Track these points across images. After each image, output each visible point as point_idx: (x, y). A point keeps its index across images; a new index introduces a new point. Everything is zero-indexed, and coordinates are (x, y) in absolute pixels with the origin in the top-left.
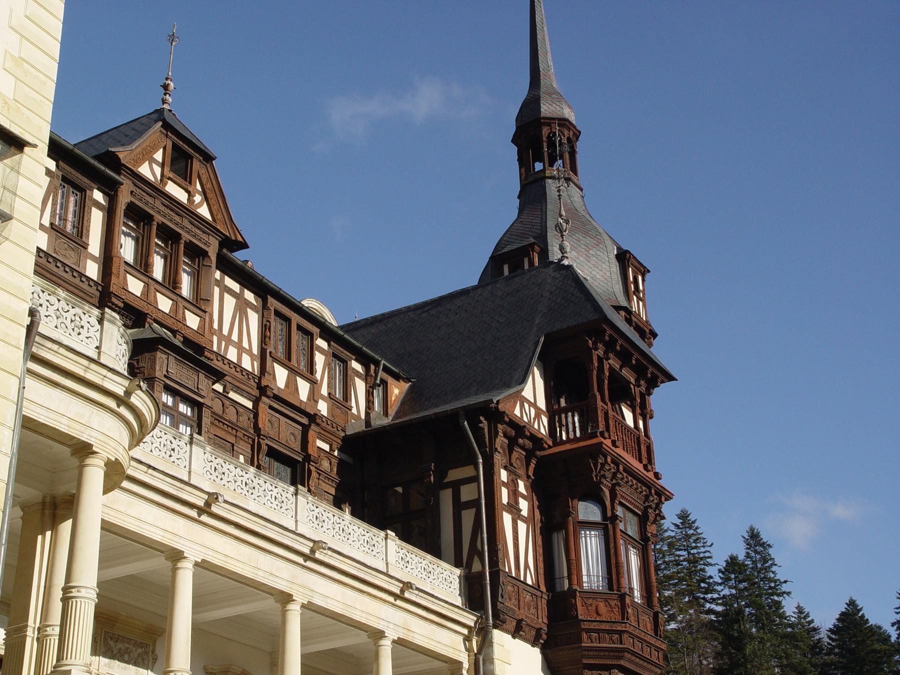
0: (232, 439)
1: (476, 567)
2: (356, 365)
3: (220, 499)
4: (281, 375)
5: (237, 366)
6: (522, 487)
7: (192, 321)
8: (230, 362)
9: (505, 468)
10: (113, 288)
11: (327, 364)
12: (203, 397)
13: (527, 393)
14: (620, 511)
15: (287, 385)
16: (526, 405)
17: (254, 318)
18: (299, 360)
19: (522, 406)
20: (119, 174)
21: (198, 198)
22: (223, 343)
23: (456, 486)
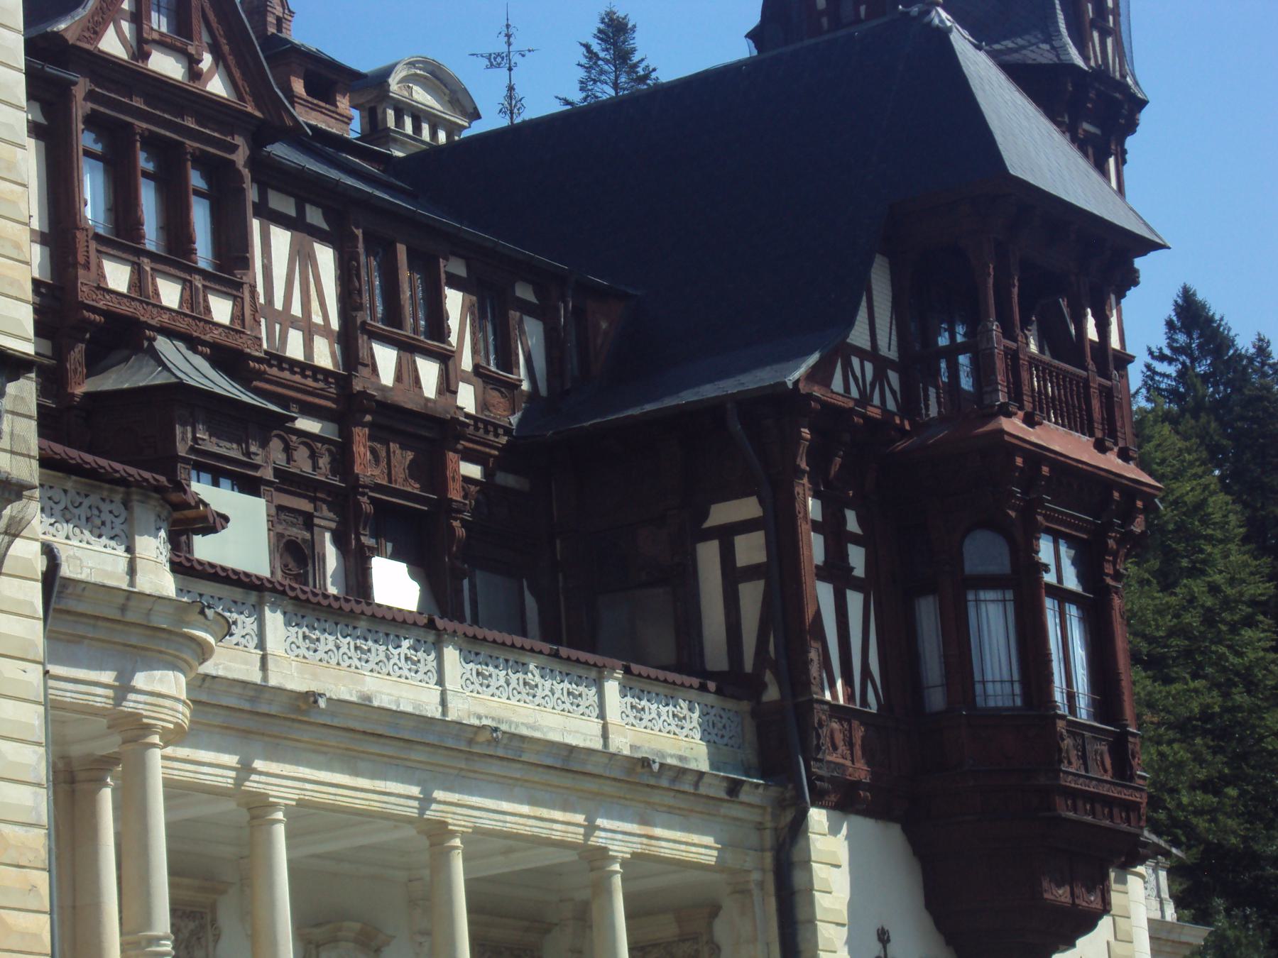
0: (305, 506)
1: (772, 693)
2: (524, 292)
3: (322, 703)
4: (386, 359)
5: (306, 368)
6: (852, 525)
7: (221, 310)
8: (293, 363)
9: (816, 495)
10: (85, 294)
11: (466, 308)
12: (256, 467)
13: (859, 336)
14: (1045, 550)
15: (398, 378)
16: (855, 361)
17: (325, 256)
18: (414, 321)
19: (847, 366)
20: (64, 65)
21: (207, 61)
22: (278, 327)
23: (726, 534)
